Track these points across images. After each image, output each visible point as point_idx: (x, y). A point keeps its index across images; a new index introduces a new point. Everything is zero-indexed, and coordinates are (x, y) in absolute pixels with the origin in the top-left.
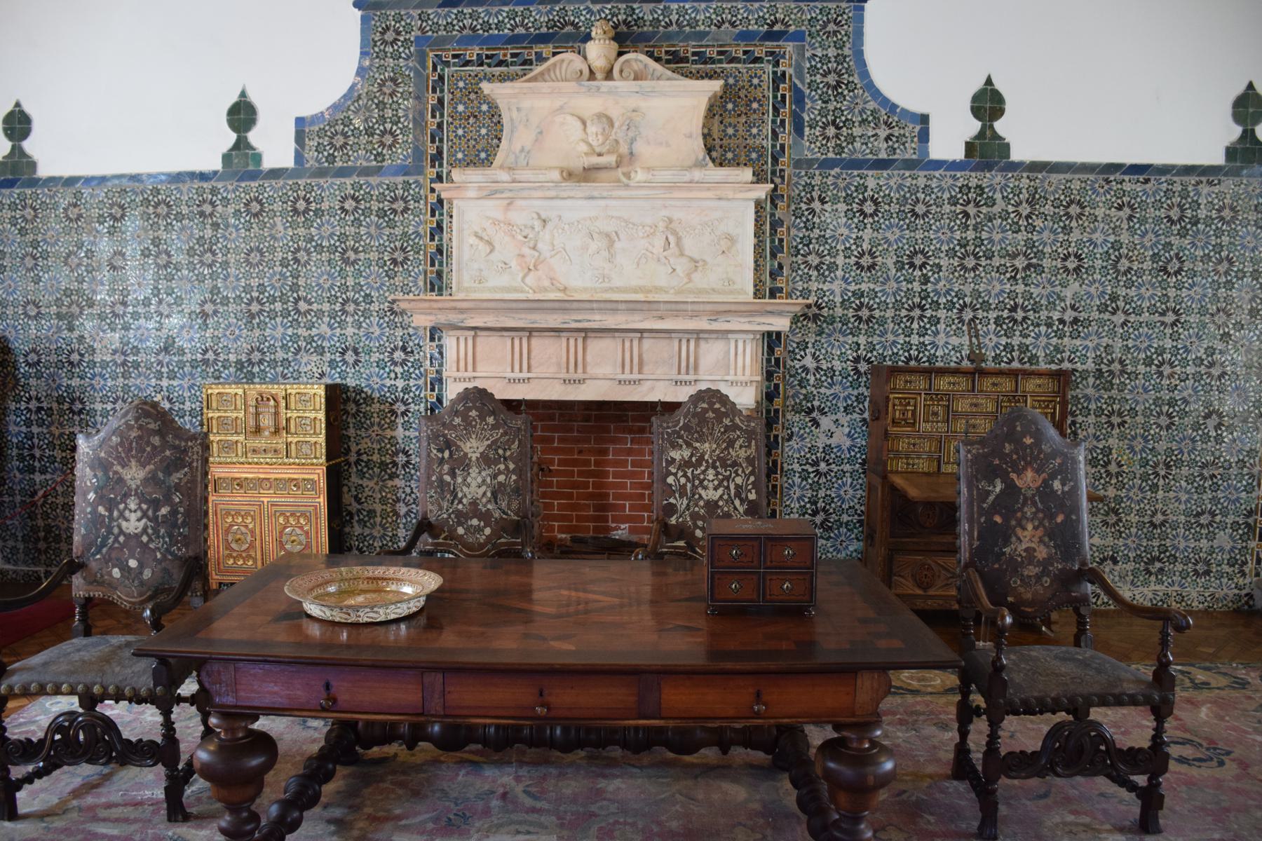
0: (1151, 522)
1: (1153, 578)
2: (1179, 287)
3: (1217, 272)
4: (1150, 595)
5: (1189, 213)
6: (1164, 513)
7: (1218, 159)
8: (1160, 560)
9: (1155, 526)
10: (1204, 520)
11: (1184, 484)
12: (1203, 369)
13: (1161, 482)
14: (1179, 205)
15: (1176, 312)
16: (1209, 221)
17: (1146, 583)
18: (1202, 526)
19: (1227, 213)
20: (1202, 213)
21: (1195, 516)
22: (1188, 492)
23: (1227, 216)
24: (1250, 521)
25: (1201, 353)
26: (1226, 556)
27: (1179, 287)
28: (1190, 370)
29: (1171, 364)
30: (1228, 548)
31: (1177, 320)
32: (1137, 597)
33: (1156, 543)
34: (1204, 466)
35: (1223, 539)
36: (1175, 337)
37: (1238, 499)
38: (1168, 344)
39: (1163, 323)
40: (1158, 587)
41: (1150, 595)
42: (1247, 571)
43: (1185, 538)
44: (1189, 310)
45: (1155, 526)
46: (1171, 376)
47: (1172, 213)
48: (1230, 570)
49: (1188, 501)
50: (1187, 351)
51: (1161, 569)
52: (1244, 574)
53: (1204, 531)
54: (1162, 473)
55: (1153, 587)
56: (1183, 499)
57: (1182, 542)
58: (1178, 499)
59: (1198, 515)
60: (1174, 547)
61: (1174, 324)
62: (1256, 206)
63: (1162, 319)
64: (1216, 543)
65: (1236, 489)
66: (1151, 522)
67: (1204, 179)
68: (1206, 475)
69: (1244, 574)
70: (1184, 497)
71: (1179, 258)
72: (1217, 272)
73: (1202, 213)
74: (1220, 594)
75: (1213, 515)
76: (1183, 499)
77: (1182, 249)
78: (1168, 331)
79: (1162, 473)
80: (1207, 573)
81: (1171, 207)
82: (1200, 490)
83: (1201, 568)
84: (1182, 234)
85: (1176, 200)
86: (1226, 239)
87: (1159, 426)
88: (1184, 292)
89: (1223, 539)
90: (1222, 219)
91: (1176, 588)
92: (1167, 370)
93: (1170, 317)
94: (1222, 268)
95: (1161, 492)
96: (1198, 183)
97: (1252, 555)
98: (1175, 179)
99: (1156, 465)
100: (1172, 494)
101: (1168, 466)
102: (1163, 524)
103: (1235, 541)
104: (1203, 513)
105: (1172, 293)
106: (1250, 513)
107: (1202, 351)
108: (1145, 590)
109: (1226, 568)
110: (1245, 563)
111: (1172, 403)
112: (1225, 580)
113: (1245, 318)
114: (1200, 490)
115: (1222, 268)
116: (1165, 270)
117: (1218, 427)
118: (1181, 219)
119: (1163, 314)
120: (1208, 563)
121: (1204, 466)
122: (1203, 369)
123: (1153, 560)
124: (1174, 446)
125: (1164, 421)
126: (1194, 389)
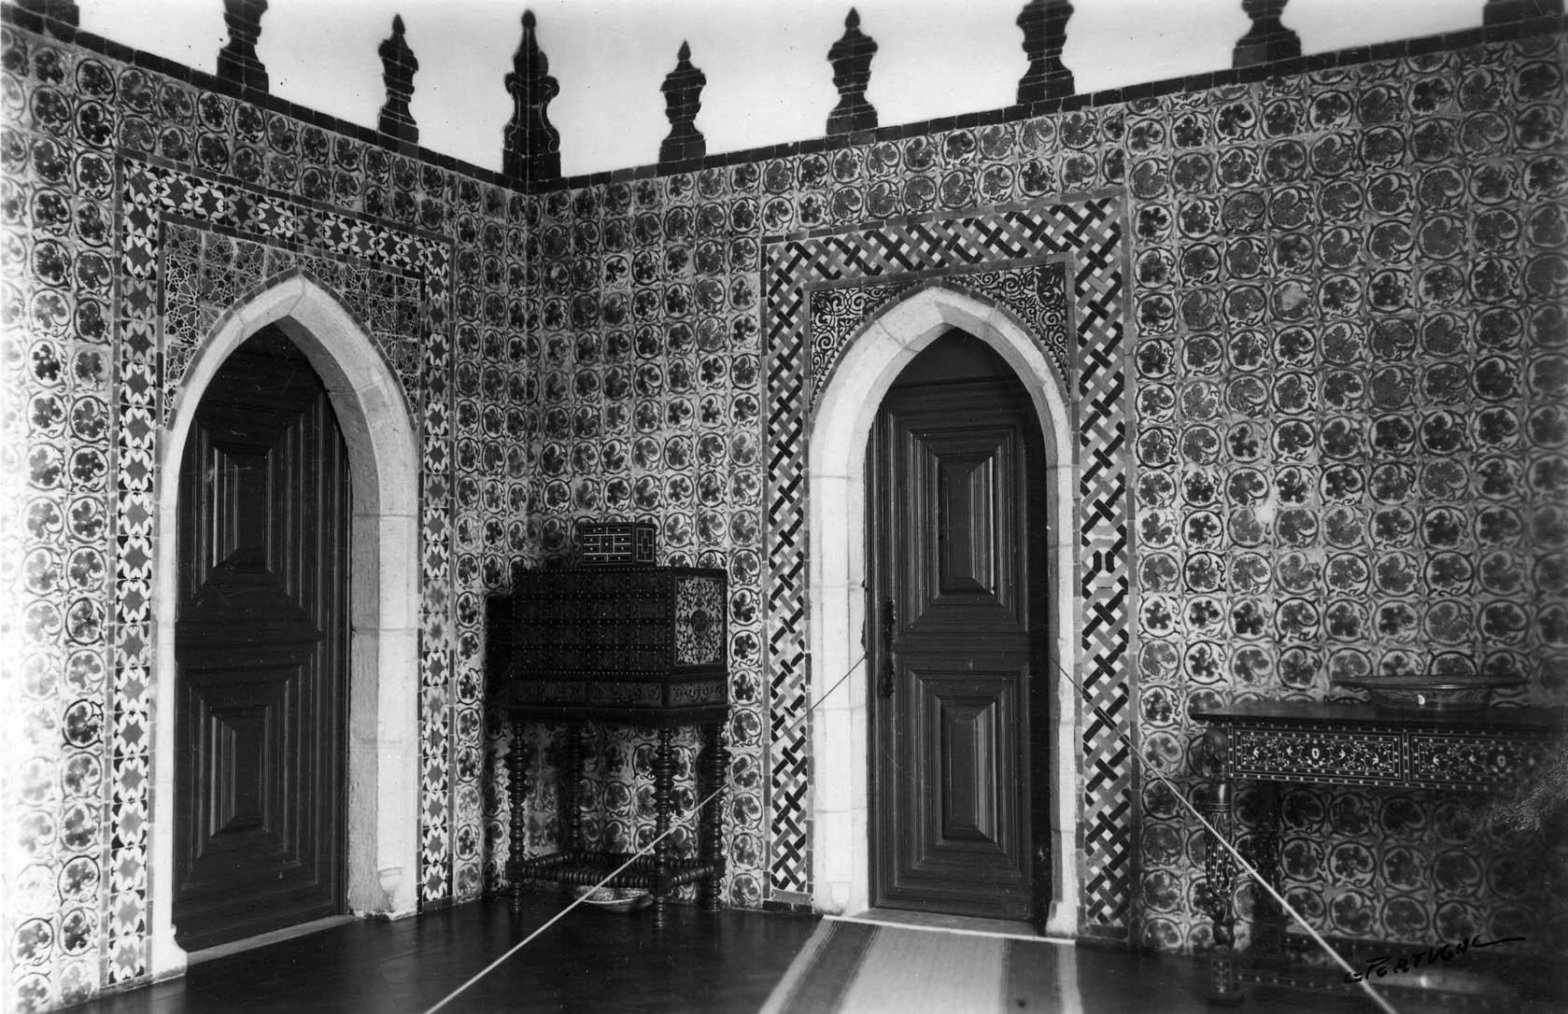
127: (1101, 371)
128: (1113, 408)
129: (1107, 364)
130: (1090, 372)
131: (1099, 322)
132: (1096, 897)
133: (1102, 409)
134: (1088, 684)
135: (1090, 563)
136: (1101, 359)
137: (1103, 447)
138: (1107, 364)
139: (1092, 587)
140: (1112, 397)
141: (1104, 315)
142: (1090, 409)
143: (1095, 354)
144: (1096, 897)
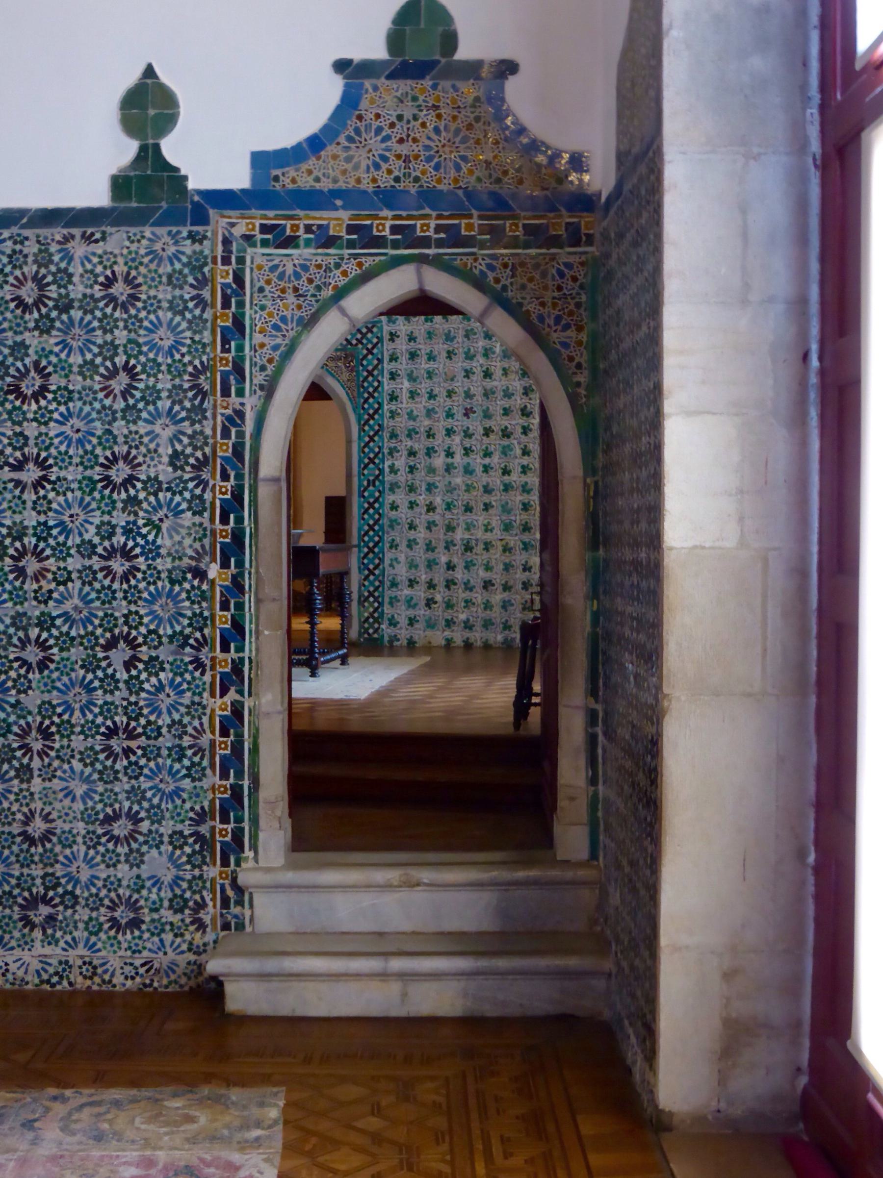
0: (24, 834)
1: (38, 934)
2: (43, 419)
3: (109, 392)
4: (35, 965)
5: (53, 291)
6: (46, 818)
7: (98, 196)
8: (47, 902)
9: (32, 842)
10: (121, 828)
11: (77, 765)
12: (96, 563)
13: (36, 763)
14: (35, 278)
15: (42, 464)
16: (88, 304)
17: (26, 943)
18: (117, 840)
19: (120, 289)
20: (77, 290)
21: (102, 823)
22: (87, 780)
23: (120, 294)
24: (204, 829)
25: (91, 534)
26: (166, 894)
27: (43, 419)
28: (74, 563)
29: (38, 555)
30: (168, 879)
31: (44, 478)
32: (13, 967)
33: (37, 871)
34: (112, 732)
35: (157, 863)
36: (42, 506)
37: (177, 792)
38: (31, 519)
39: (18, 483)
40: (48, 950)
41: (35, 965)
42: (207, 919)
43: (89, 861)
44: (64, 459)
45: (32, 842)
46: (38, 577)
47: (23, 292)
48: (176, 919)
49: (87, 796)
50: (66, 531)
51: (51, 918)
52: (201, 926)
53: (122, 850)
54: (37, 746)
55: (39, 949)
56: (79, 792)
57: (85, 870)
58: (69, 793)
59: (109, 820)
60: (70, 877)
61: (38, 484)
62: (170, 277)
63: (15, 475)
64: (145, 871)
65: (172, 774)
66: (24, 834)
67: (77, 232)
68: (118, 749)
69: (201, 926)
70: (80, 789)
71: (40, 370)
72: (109, 392)
73: (77, 290)
74: (161, 960)
75: (136, 820)
76: (79, 792)
77: (45, 353)
78: (30, 496)
79: (37, 746)
80: (135, 923)
81: (20, 282)
82: (109, 776)
83: (122, 914)
84: (44, 327)
85: (30, 269)
86: (121, 336)
87: (24, 662)
88: (54, 429)
89: (157, 863)
90: (112, 299)
91: (81, 951)
92: (32, 565)
93: (31, 474)
94: (121, 382)
95: (37, 781)
96: (67, 239)
97: (213, 891)
98: (26, 233)
99: (25, 732)
100: (56, 784)
101: (46, 735)
102: (46, 837)
103: (178, 867)
104: (116, 817)
105: (31, 430)
106: (202, 817)
107: (92, 530)
108: (26, 956)
109: (167, 915)
110: (201, 906)
111: (45, 622)
112: (168, 937)
113: (165, 472)
114: (109, 776)
115: (121, 382)
116: (16, 390)
117: (128, 665)
118: (39, 302)
119: (19, 467)
120: (133, 906)
121: (112, 732)
122: (96, 563)
123: (33, 902)
124: (55, 698)
125: (33, 654)
126: (83, 598)
127: (371, 400)
128: (376, 417)
129: (373, 397)
130: (366, 401)
131: (370, 379)
132: (366, 625)
133: (372, 417)
134: (364, 535)
135: (365, 483)
136: (371, 395)
137: (372, 433)
138: (373, 397)
139: (366, 494)
140: (376, 411)
141: (373, 376)
142: (366, 417)
143: (369, 393)
144: (366, 625)
